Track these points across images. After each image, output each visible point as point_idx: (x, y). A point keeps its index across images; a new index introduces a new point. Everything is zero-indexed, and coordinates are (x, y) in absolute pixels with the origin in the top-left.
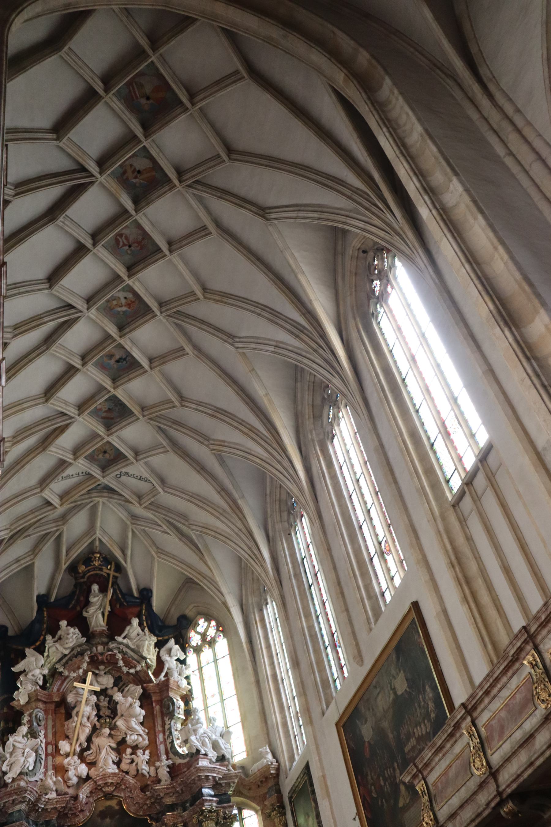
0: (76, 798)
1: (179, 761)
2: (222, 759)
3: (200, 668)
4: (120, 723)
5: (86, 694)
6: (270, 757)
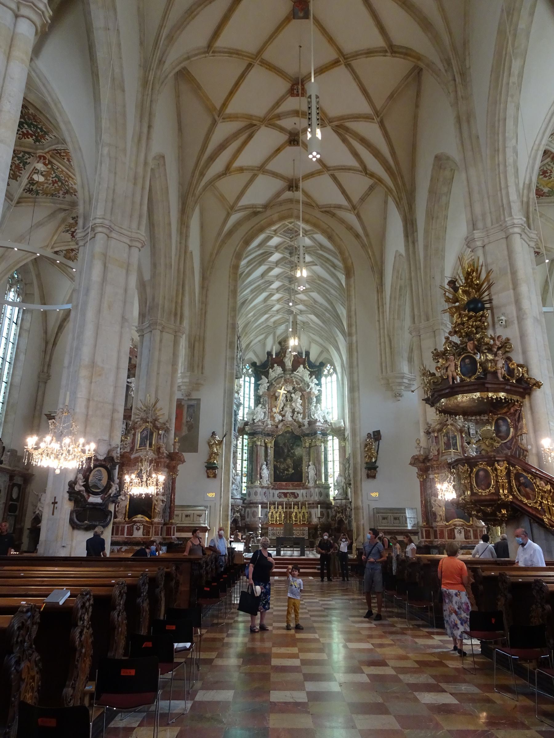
0: (277, 427)
1: (312, 420)
2: (326, 421)
3: (326, 383)
4: (293, 404)
5: (281, 394)
6: (342, 423)
